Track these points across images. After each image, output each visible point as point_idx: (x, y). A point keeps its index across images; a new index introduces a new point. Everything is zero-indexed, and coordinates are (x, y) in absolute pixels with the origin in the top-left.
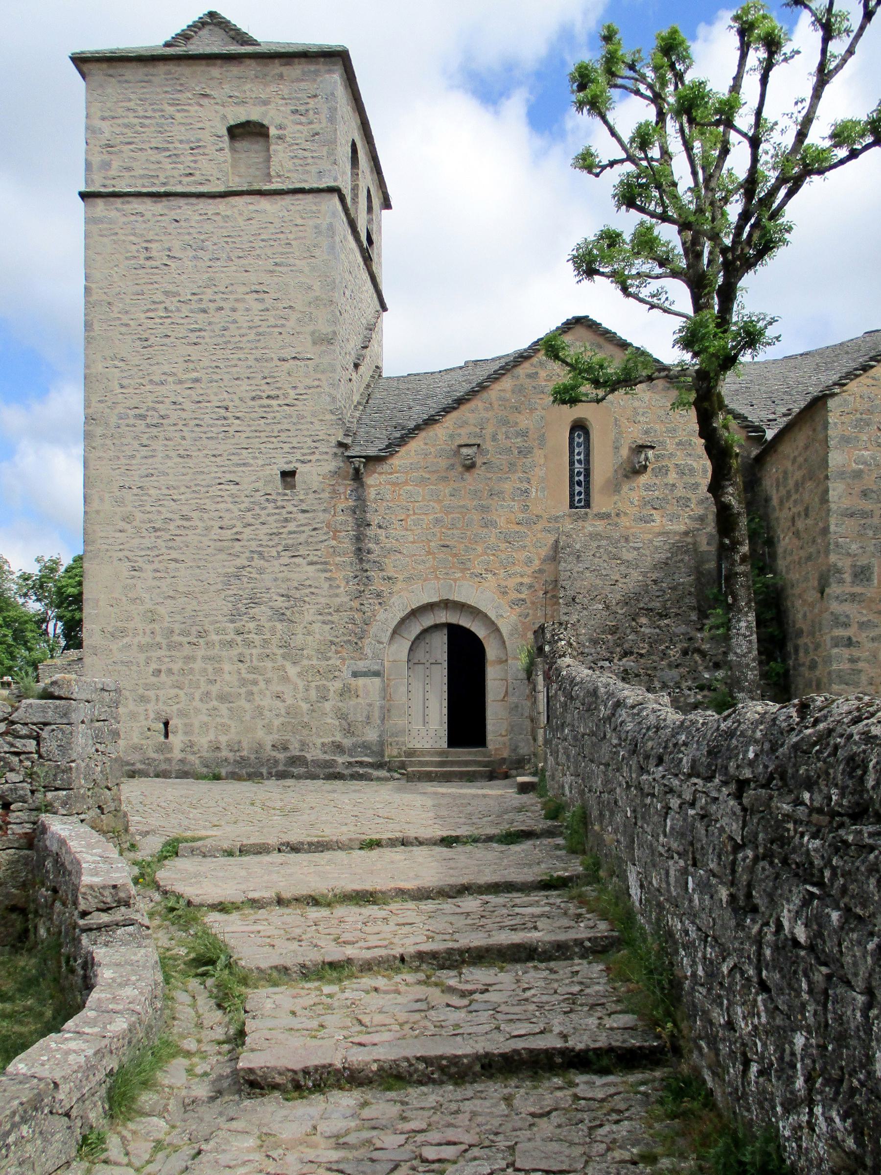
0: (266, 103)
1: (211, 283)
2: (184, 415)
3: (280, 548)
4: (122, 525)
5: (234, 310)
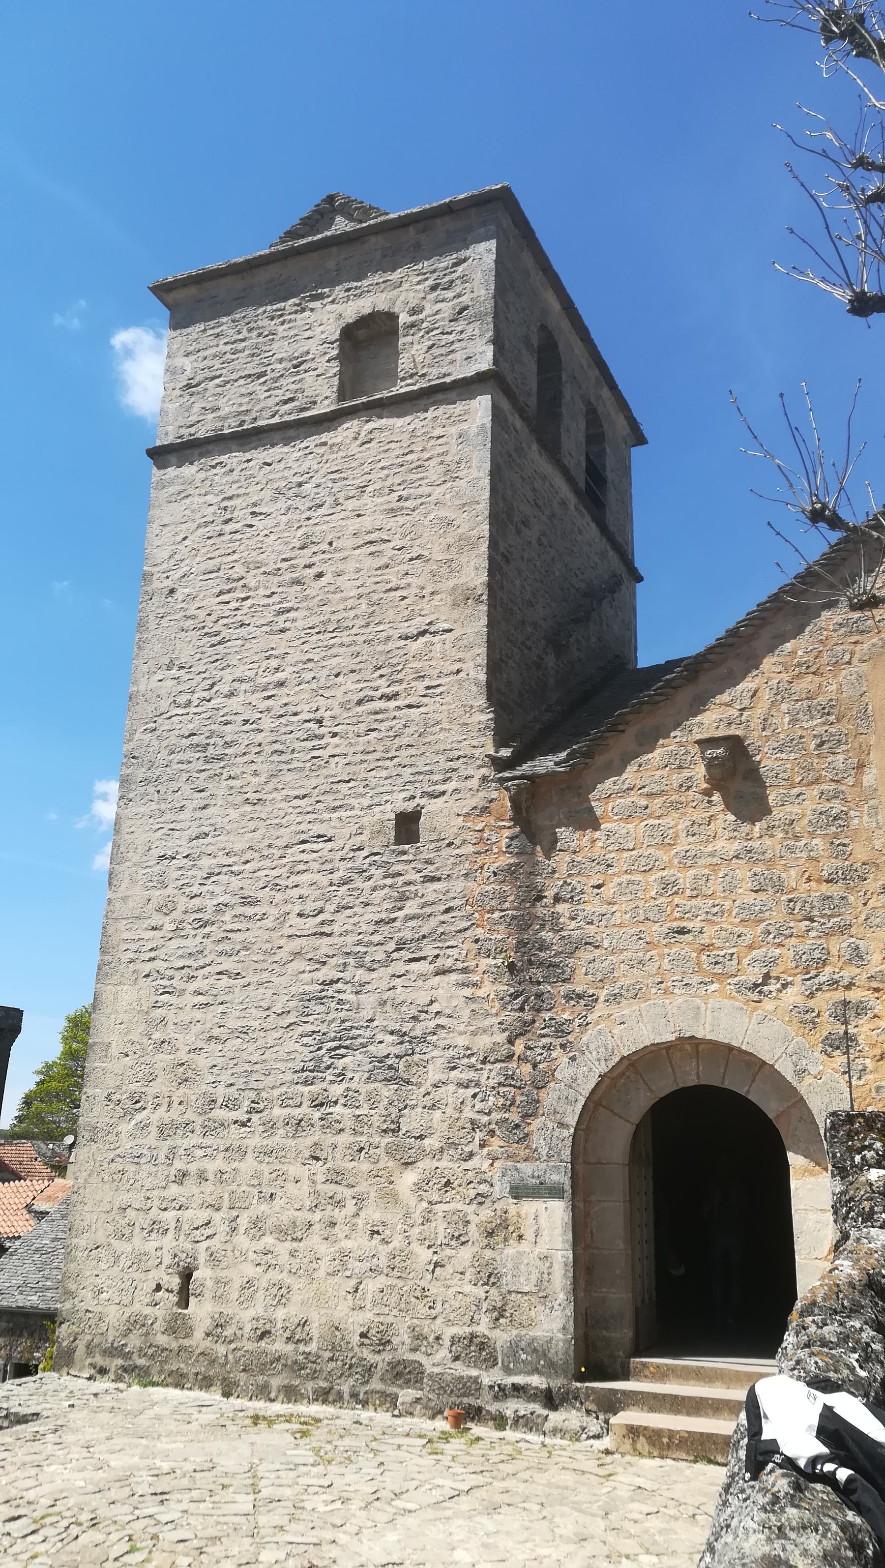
3: (392, 946)
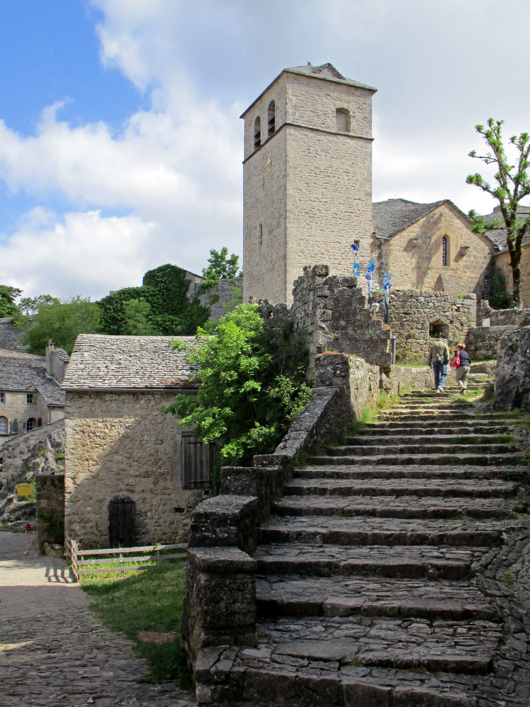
0: (349, 102)
1: (331, 166)
2: (322, 215)
4: (300, 254)
5: (339, 178)
